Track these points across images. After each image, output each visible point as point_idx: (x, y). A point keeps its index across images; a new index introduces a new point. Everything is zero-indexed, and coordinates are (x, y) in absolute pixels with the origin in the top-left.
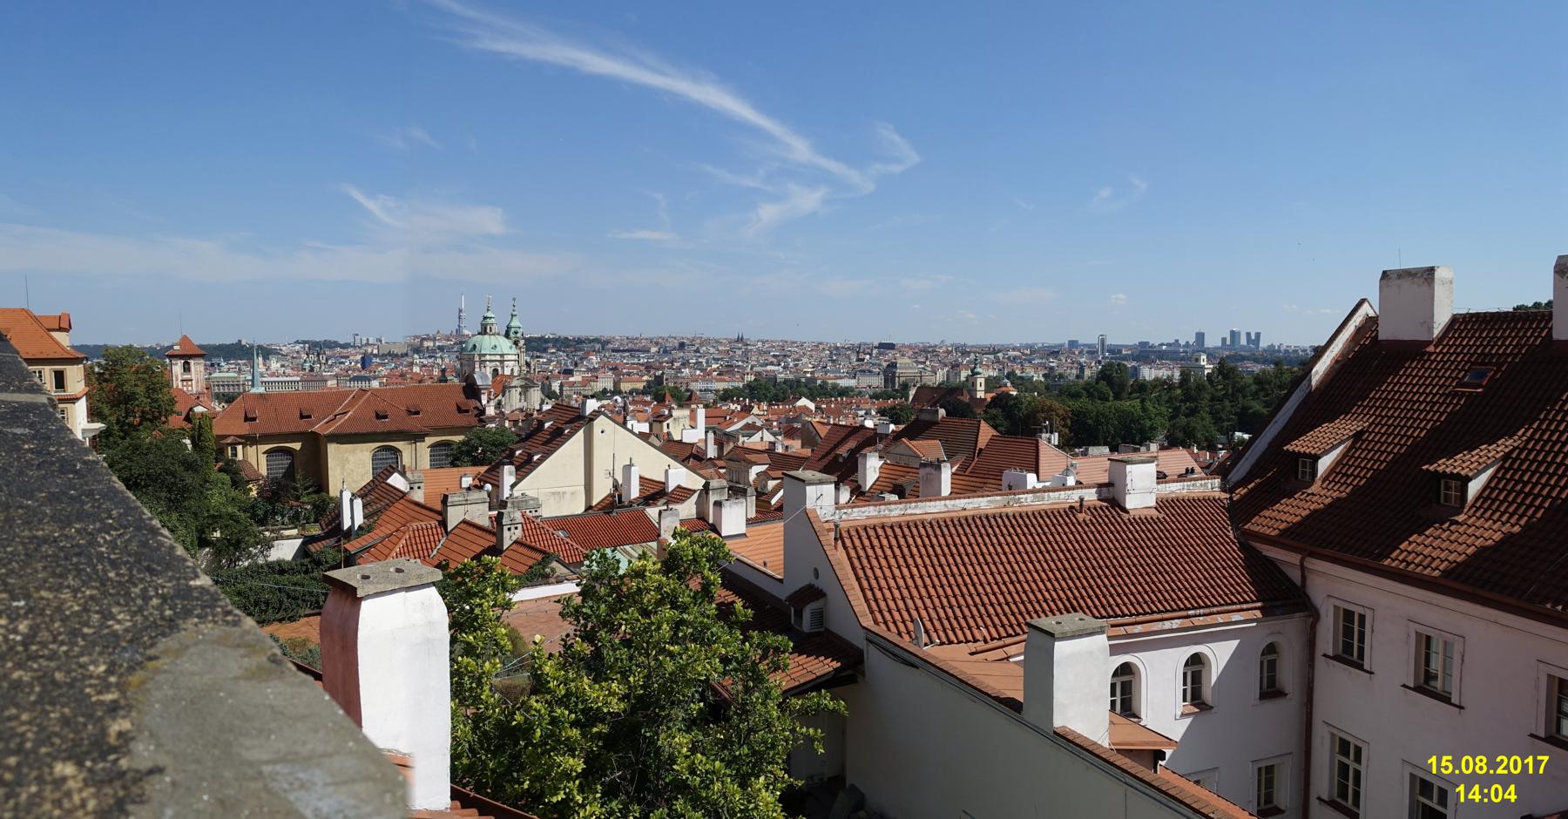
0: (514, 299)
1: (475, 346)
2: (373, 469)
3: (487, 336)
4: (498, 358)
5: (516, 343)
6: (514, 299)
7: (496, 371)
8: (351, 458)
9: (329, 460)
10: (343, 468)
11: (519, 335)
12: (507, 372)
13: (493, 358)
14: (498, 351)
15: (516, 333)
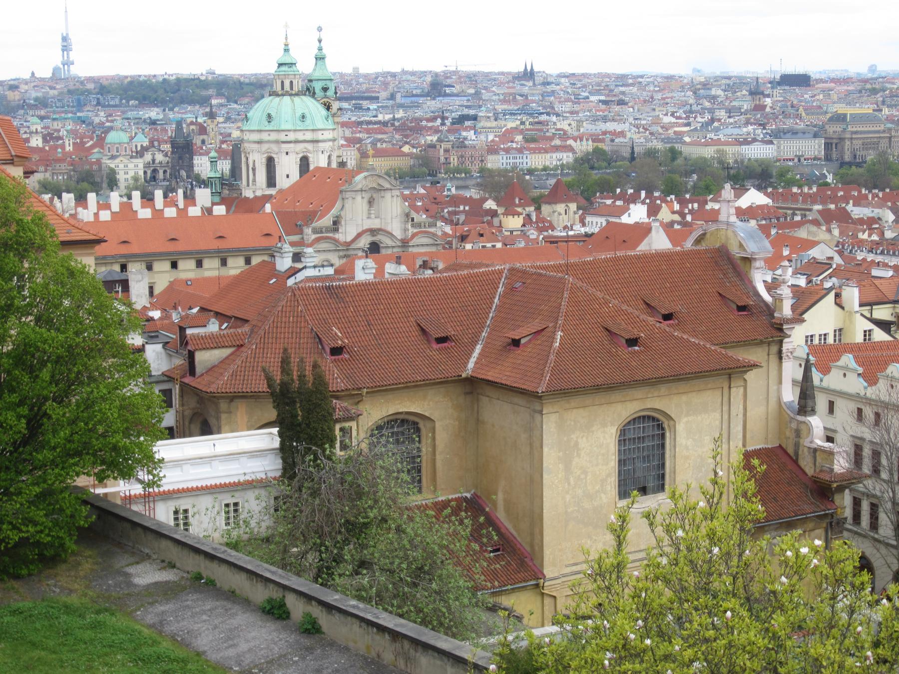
0: (320, 29)
1: (269, 116)
2: (621, 462)
3: (287, 99)
4: (309, 136)
5: (328, 107)
6: (320, 29)
7: (304, 162)
8: (583, 443)
9: (546, 450)
10: (568, 469)
11: (330, 93)
12: (323, 162)
13: (300, 136)
14: (308, 124)
15: (325, 89)
